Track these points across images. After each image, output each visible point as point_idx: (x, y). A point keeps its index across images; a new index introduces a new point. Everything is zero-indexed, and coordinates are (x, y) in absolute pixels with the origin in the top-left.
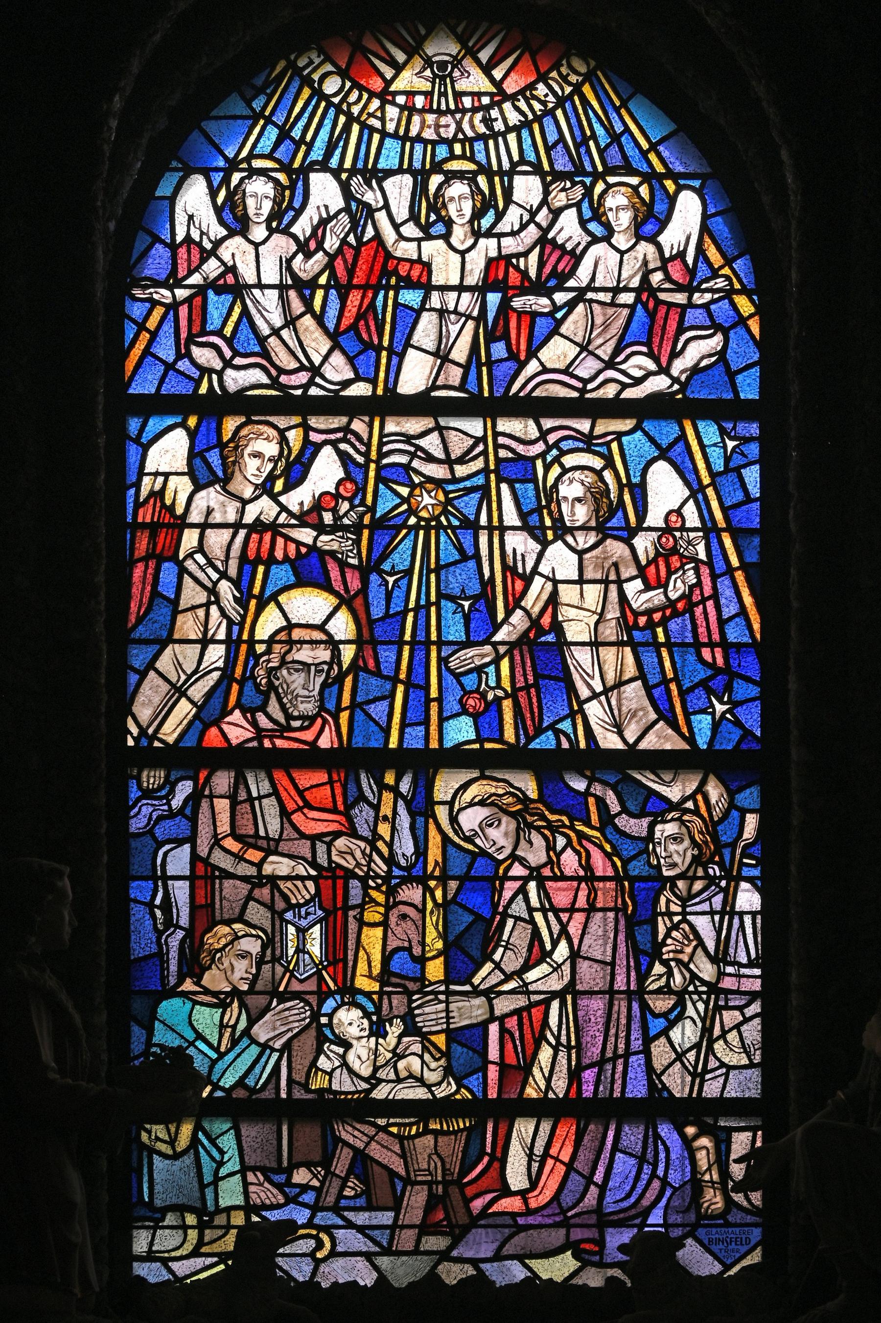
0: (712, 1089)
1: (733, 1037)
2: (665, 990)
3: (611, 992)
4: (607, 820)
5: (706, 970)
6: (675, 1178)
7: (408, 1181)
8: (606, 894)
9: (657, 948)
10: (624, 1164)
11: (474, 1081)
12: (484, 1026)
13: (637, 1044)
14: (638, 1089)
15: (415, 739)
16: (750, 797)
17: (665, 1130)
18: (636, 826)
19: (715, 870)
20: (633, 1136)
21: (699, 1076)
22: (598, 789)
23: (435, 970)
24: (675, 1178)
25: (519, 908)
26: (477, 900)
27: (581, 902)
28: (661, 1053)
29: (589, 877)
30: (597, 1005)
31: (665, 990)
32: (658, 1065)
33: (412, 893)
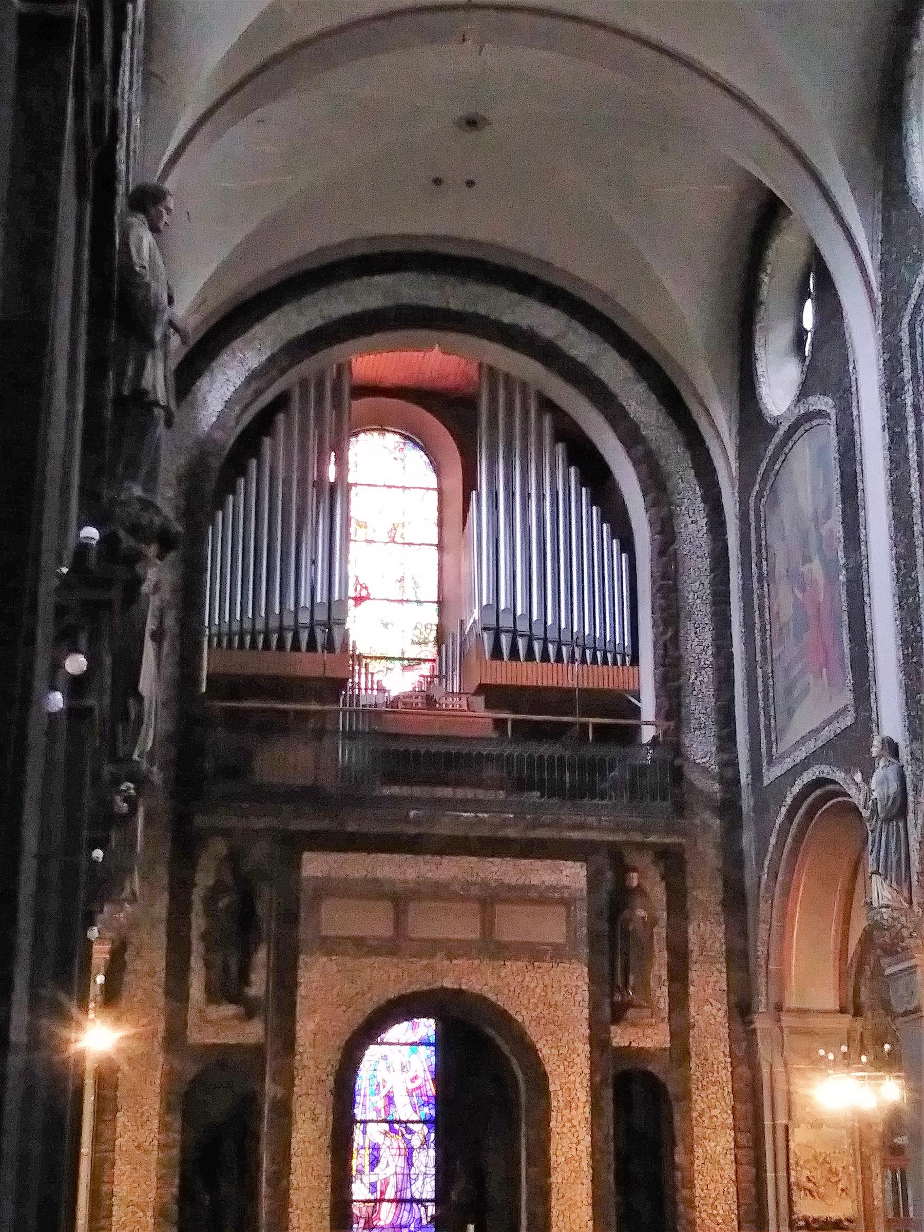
0: (424, 1197)
1: (429, 1184)
2: (415, 1174)
3: (403, 1174)
4: (403, 1135)
5: (423, 1169)
6: (416, 1217)
7: (361, 1217)
8: (403, 1152)
9: (413, 1165)
10: (406, 1214)
11: (375, 1194)
12: (376, 1182)
13: (409, 1186)
14: (409, 1197)
15: (363, 1118)
16: (433, 1130)
17: (414, 1205)
18: (408, 1136)
19: (425, 1146)
20: (408, 1206)
21: (421, 1193)
22: (401, 1128)
23: (367, 1169)
24: (416, 1217)
25: (384, 1155)
26: (375, 1153)
27: (398, 1154)
28: (413, 1188)
29: (399, 1148)
30: (400, 1177)
31: (415, 1174)
32: (413, 1191)
33: (362, 1151)
